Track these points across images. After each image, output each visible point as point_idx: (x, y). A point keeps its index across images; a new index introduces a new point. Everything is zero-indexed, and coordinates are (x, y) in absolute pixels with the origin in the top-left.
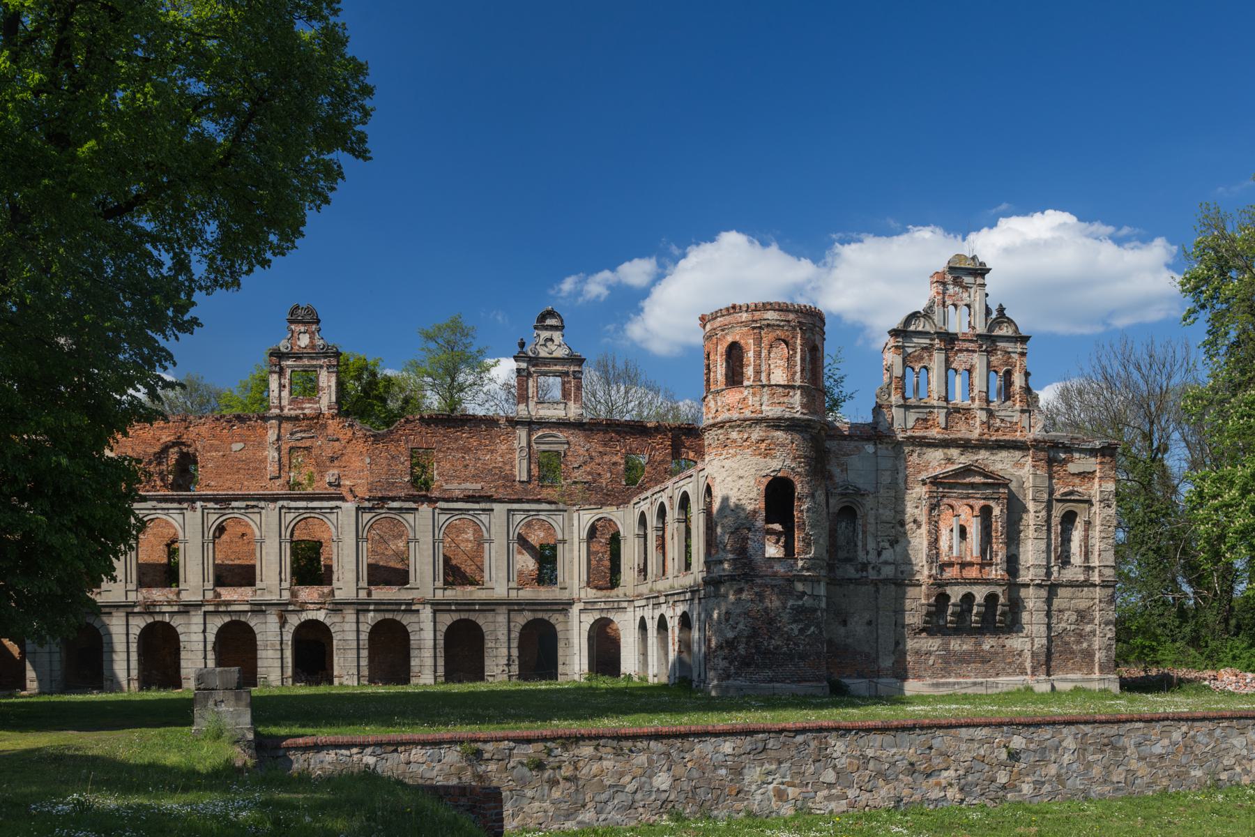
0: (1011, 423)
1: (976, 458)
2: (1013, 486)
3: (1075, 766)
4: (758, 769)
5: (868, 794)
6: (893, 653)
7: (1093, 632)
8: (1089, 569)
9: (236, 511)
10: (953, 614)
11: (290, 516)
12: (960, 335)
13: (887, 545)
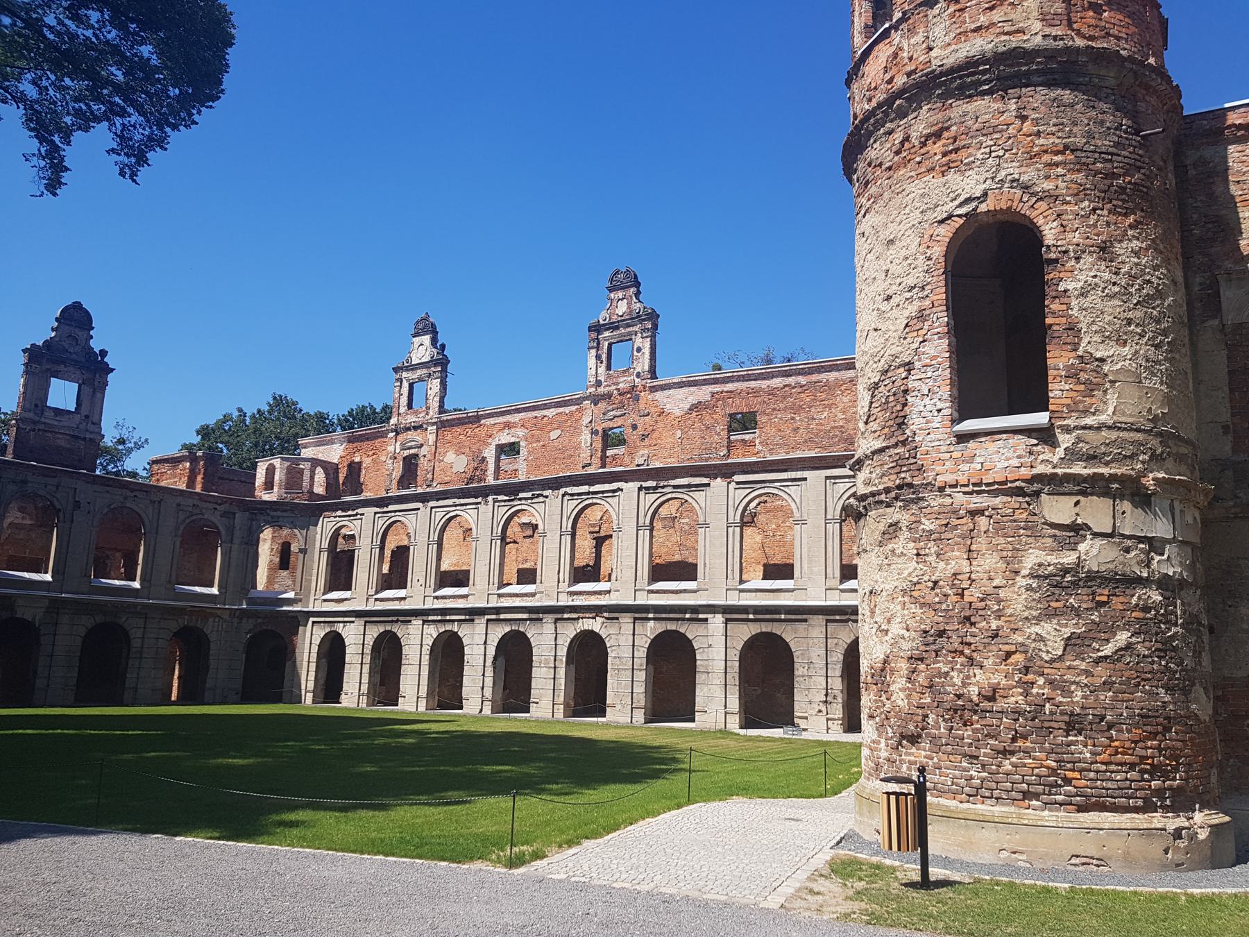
9: (523, 502)
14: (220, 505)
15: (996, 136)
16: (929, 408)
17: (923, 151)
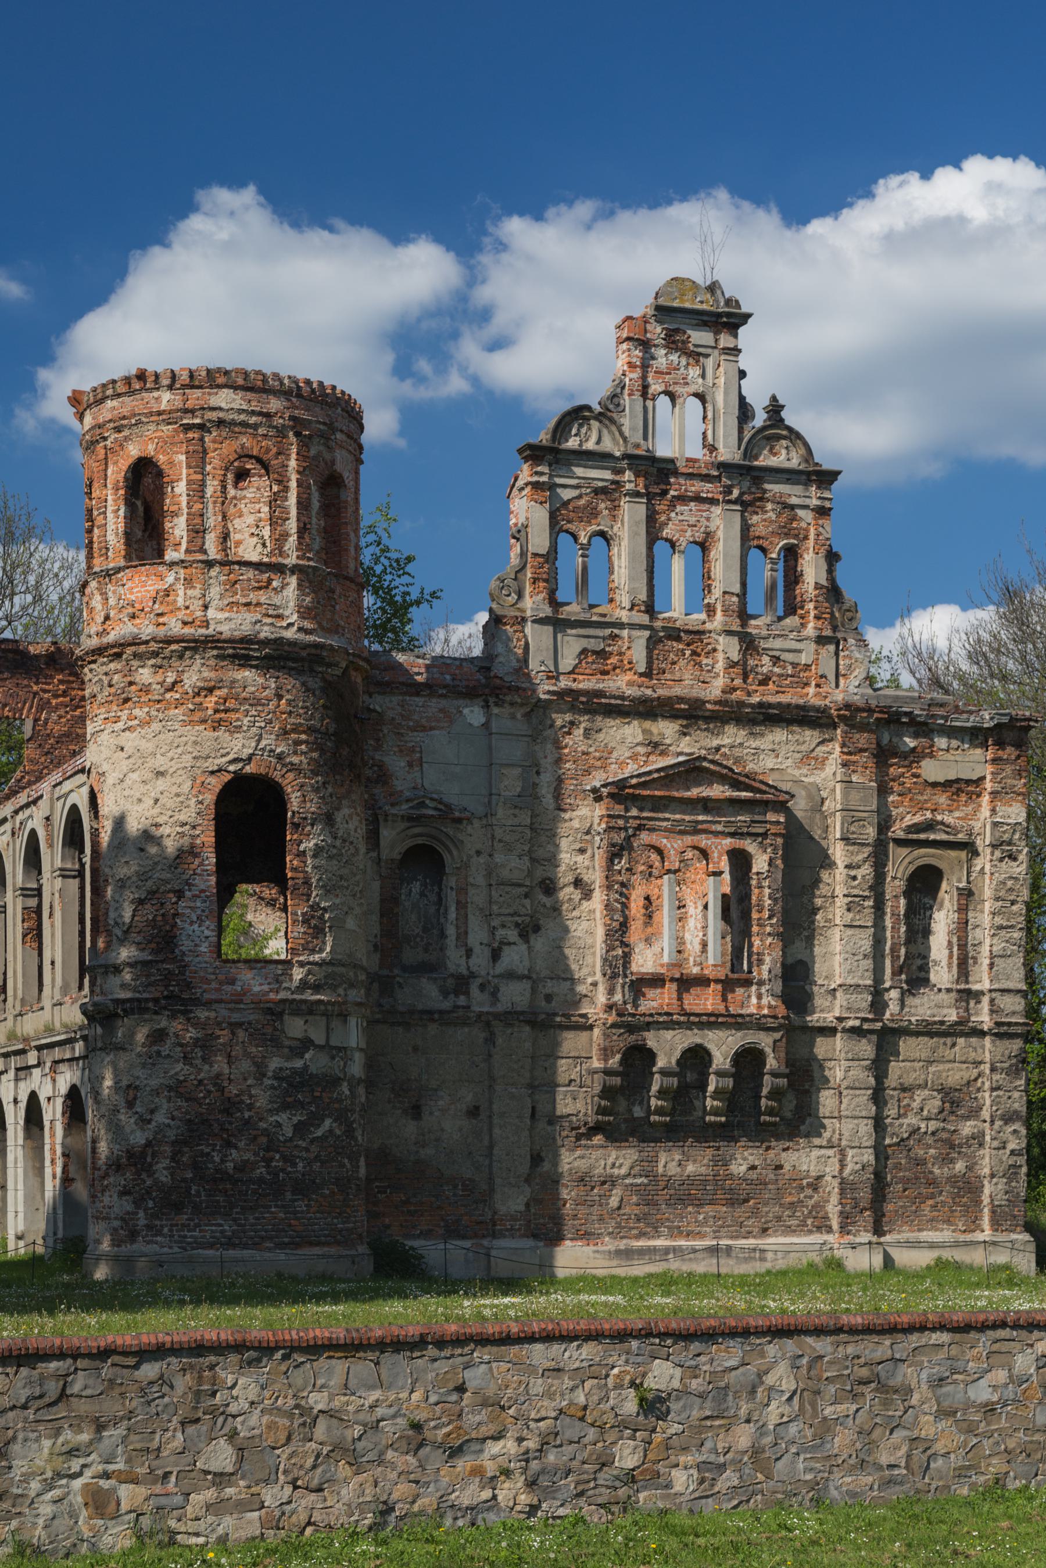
0: (795, 665)
1: (715, 743)
2: (800, 807)
3: (793, 1429)
4: (47, 1443)
5: (313, 1497)
6: (528, 1180)
7: (978, 1138)
8: (967, 996)
10: (662, 1093)
12: (680, 464)
13: (512, 935)
15: (260, 708)
16: (198, 933)
17: (197, 700)
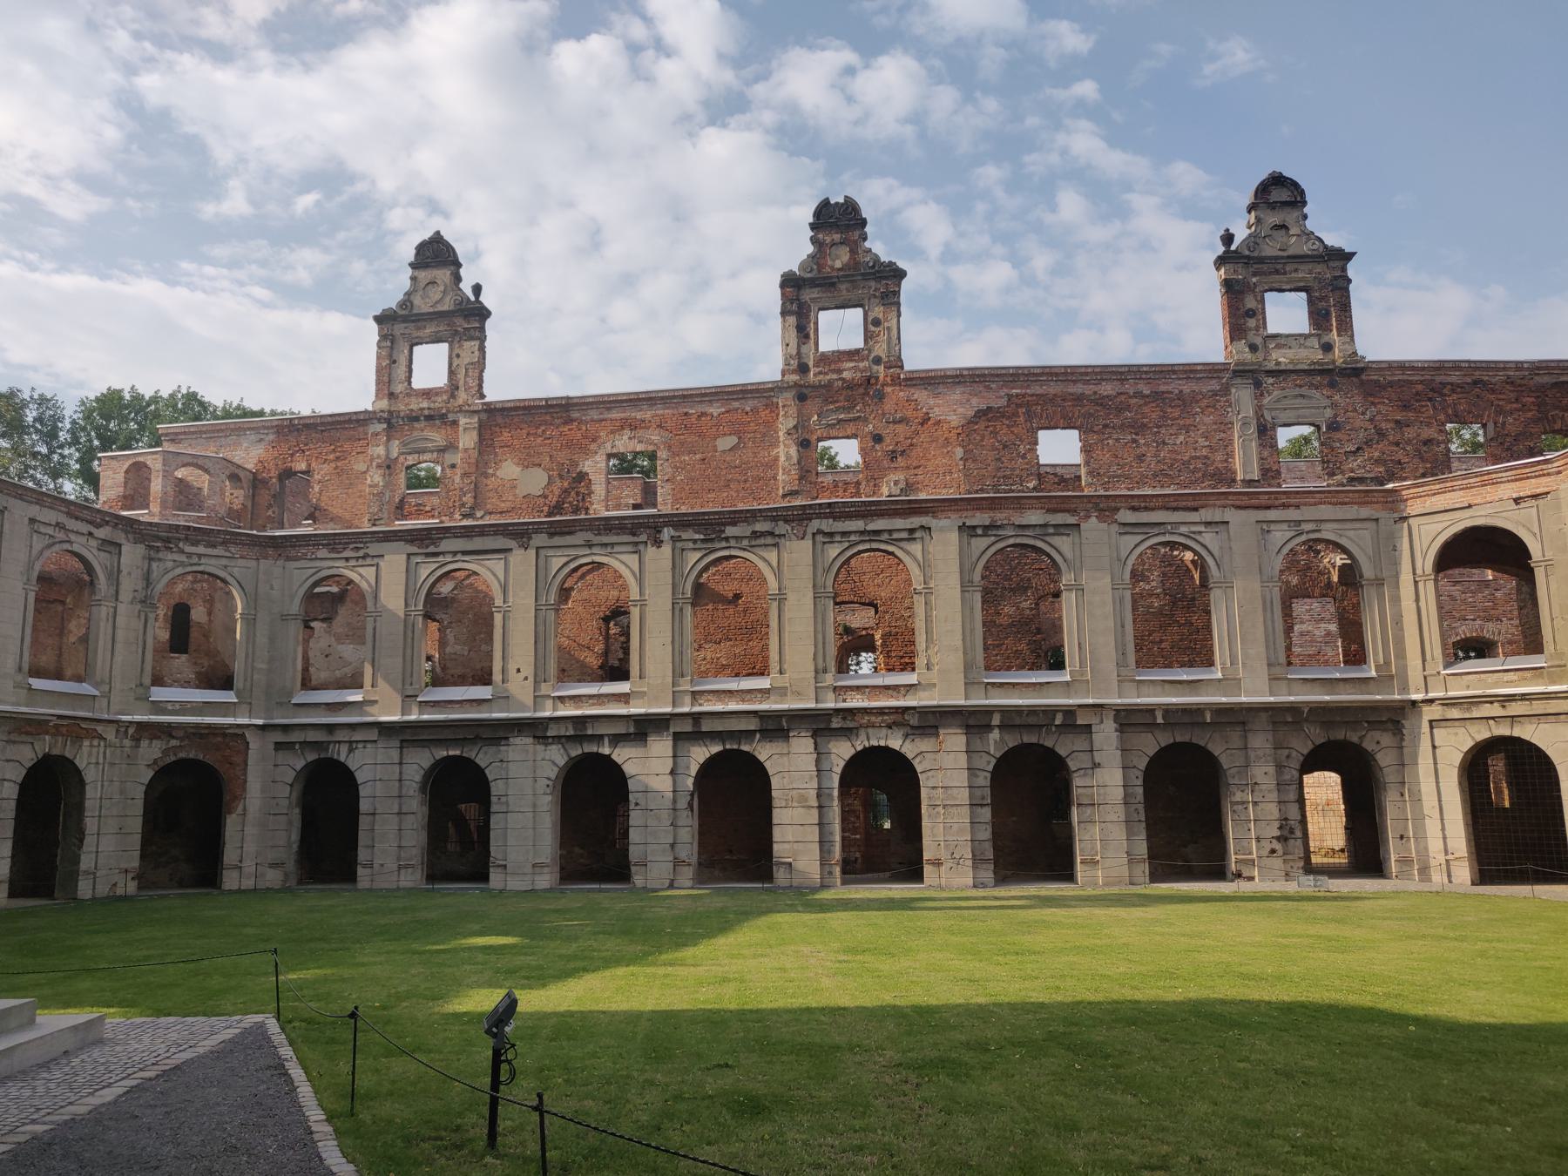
11: (833, 551)
14: (98, 526)
